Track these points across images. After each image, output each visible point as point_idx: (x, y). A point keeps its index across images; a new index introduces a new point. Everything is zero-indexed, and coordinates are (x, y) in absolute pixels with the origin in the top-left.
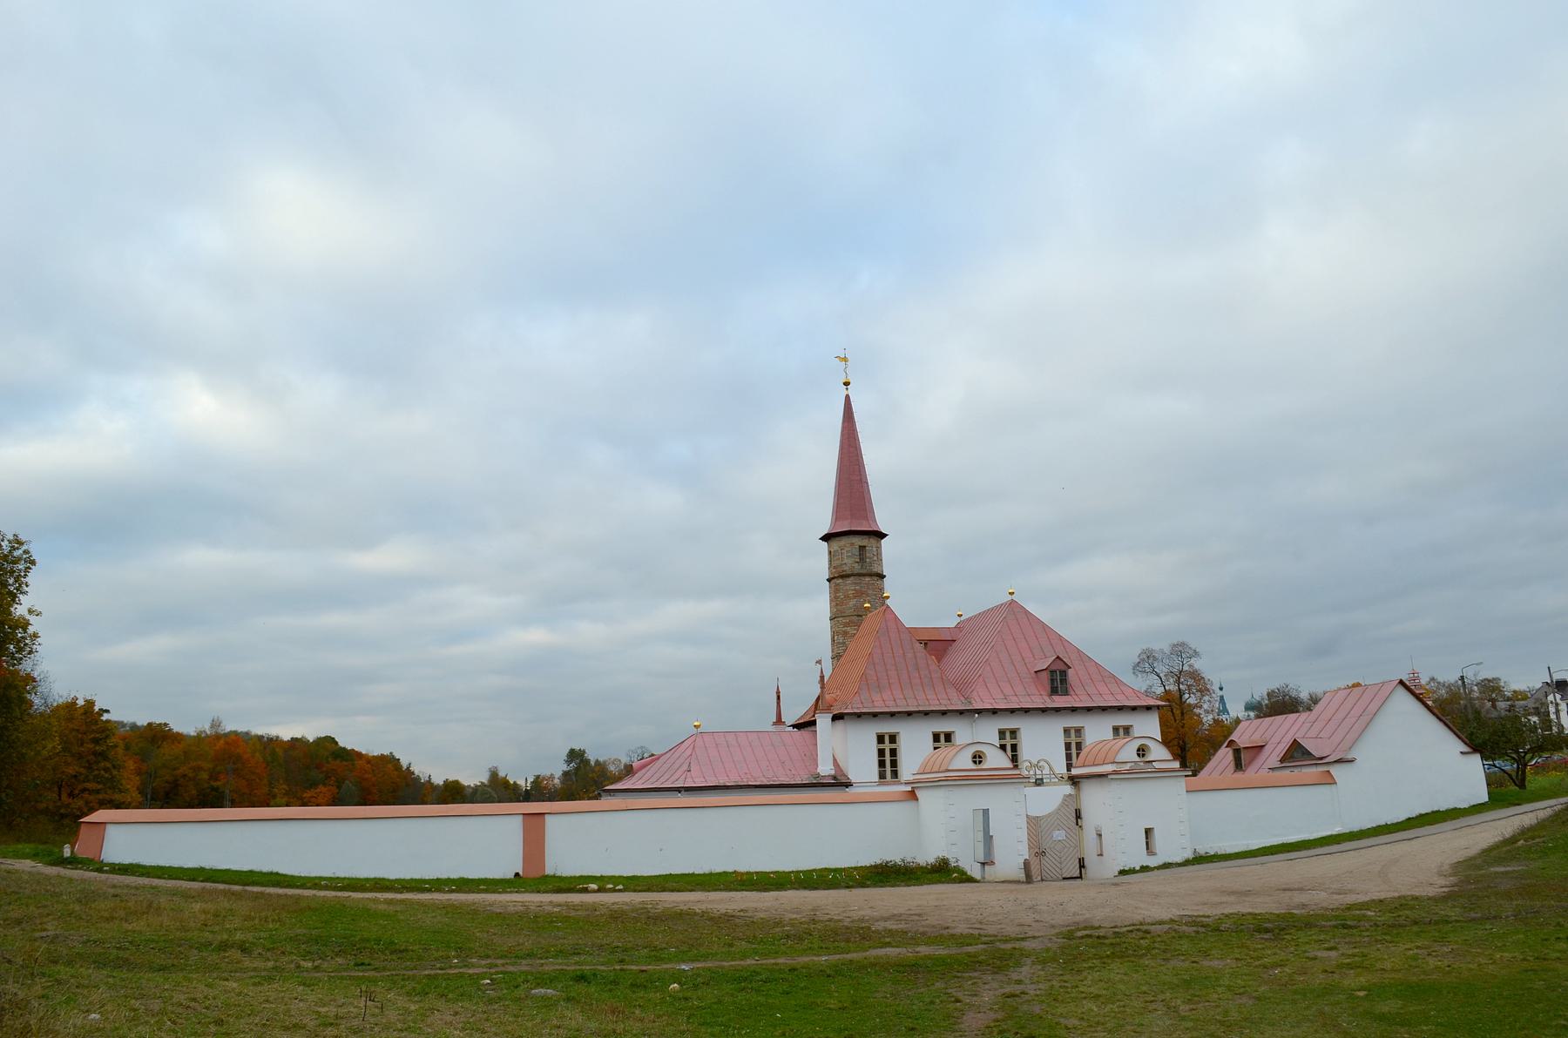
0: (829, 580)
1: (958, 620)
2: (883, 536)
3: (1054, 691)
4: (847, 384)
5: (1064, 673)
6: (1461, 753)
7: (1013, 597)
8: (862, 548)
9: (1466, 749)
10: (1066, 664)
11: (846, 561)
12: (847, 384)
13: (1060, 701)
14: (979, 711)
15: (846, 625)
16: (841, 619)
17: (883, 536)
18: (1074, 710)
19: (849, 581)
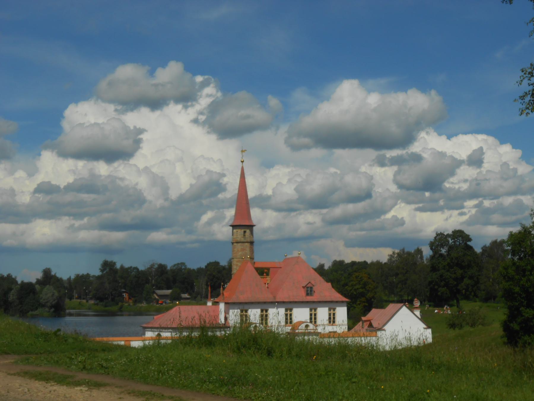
0: (233, 243)
1: (285, 257)
2: (254, 226)
3: (307, 294)
4: (242, 162)
5: (311, 288)
6: (425, 328)
7: (300, 255)
8: (245, 232)
9: (425, 326)
10: (312, 284)
11: (238, 236)
12: (242, 162)
13: (309, 298)
14: (278, 302)
15: (237, 262)
16: (236, 259)
17: (254, 226)
18: (314, 302)
19: (239, 244)
